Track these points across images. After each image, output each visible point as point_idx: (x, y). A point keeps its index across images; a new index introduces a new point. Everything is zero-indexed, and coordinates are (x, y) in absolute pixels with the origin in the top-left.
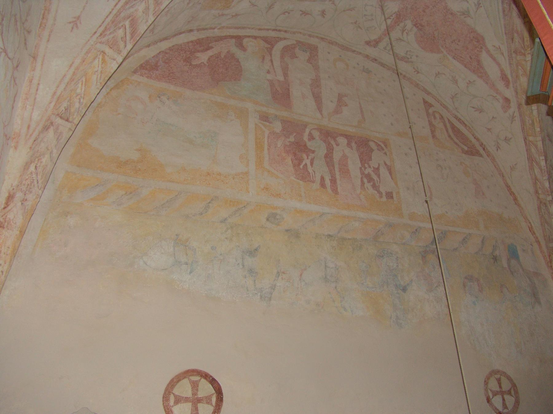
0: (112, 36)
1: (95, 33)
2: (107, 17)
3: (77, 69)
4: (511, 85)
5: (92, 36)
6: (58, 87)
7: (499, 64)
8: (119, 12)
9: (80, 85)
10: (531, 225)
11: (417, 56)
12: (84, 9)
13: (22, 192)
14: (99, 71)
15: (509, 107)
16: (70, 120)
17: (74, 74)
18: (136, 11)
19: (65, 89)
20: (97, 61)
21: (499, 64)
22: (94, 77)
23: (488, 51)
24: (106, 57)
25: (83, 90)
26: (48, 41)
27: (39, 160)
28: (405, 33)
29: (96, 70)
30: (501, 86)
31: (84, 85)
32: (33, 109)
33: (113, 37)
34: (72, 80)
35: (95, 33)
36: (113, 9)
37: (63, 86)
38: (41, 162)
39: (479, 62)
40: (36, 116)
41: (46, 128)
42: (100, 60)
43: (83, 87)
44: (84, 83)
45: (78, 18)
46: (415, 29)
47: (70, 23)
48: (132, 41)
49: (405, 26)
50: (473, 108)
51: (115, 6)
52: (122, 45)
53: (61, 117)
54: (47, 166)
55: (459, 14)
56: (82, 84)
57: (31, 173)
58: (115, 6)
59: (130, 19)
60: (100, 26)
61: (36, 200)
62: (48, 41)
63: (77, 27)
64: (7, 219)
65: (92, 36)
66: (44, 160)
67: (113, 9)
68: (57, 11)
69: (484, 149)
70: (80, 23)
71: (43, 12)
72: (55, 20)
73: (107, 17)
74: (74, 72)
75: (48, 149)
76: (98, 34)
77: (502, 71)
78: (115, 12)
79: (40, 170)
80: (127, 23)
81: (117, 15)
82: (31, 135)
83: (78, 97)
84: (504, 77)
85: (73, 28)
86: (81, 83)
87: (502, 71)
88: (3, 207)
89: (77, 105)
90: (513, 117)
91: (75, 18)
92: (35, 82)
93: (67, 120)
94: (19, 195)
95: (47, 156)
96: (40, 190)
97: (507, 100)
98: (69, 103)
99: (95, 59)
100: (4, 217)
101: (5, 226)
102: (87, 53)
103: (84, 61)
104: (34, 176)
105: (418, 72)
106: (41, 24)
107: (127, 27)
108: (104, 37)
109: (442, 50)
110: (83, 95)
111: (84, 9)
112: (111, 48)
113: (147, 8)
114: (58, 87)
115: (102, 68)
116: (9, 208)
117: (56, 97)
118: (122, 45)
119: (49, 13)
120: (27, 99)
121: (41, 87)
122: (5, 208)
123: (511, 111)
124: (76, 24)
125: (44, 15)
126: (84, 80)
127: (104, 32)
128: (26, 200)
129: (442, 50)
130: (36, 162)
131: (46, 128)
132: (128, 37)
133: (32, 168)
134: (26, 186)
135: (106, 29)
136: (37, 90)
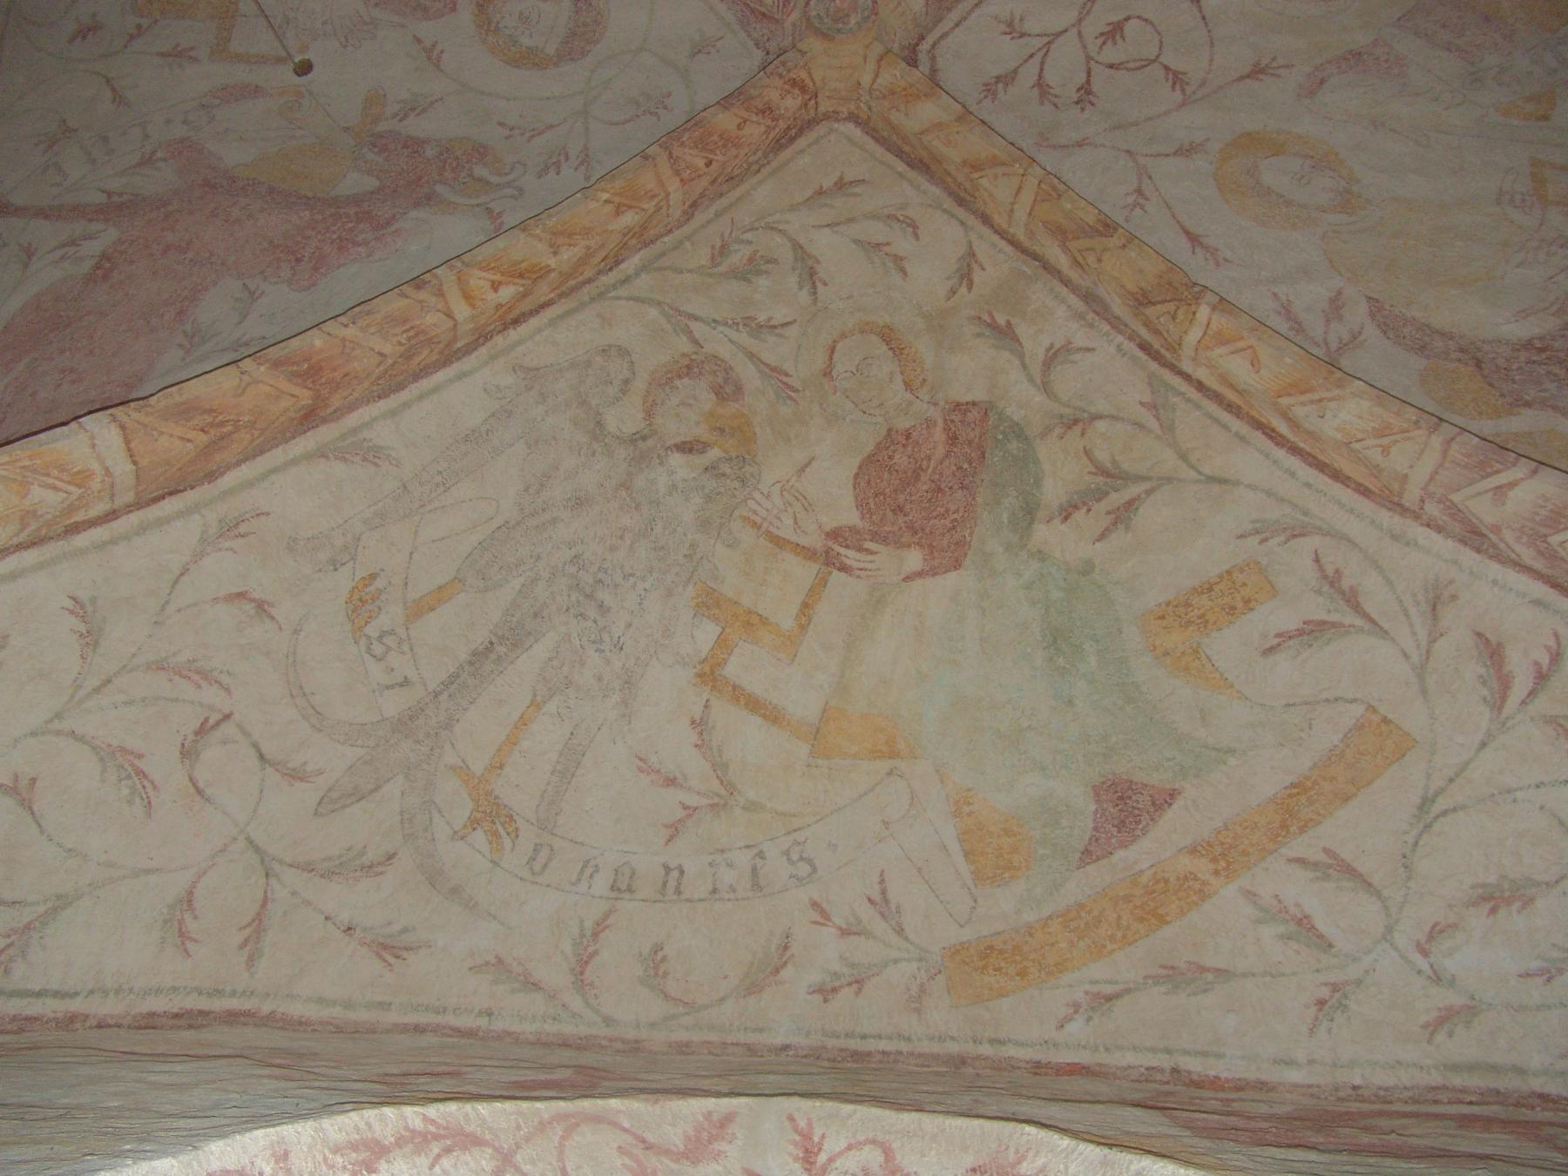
55: (188, 327)
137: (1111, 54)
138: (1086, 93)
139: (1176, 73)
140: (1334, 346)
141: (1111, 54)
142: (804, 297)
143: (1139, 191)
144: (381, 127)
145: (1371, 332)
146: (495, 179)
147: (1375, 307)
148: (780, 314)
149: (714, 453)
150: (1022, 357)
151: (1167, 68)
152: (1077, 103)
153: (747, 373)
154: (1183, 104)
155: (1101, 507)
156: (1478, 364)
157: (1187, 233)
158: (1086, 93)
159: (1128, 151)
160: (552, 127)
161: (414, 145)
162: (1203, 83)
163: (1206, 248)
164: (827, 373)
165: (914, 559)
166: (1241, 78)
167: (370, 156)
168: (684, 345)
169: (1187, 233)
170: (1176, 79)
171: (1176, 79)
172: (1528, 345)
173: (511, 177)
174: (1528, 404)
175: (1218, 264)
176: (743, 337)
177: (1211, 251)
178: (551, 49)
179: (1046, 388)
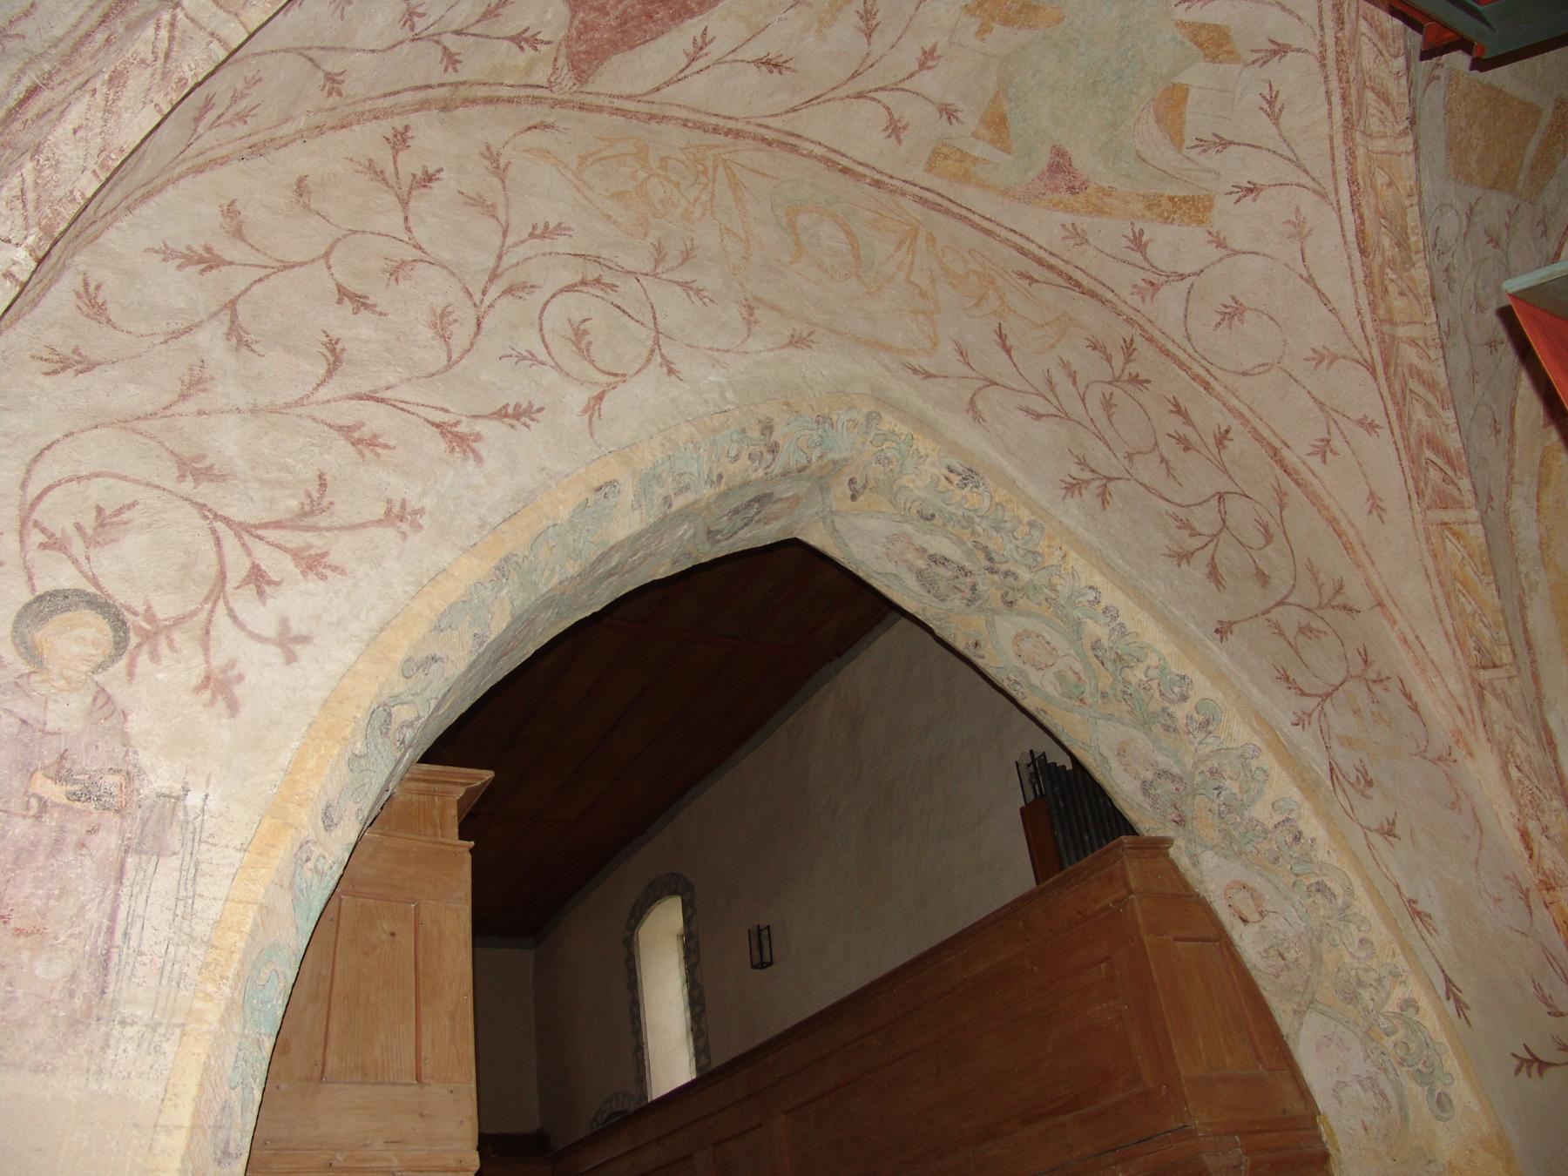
0: (1430, 490)
1: (1409, 498)
2: (1400, 460)
3: (1438, 574)
5: (1411, 507)
6: (1441, 621)
8: (1405, 438)
9: (1463, 600)
12: (1365, 476)
13: (1531, 818)
14: (1466, 556)
16: (1498, 662)
17: (1442, 584)
18: (1419, 423)
19: (1451, 616)
20: (1448, 543)
22: (1469, 571)
24: (1453, 527)
25: (1473, 603)
26: (1373, 563)
27: (1512, 753)
29: (1460, 557)
31: (1467, 595)
32: (1443, 679)
33: (1433, 490)
34: (1447, 596)
35: (1409, 498)
36: (1395, 443)
37: (1446, 615)
38: (1518, 755)
40: (1456, 688)
41: (1481, 698)
42: (1451, 537)
43: (1470, 599)
44: (1464, 591)
45: (1372, 495)
47: (1370, 512)
48: (1459, 474)
51: (1393, 434)
52: (1451, 489)
53: (1484, 668)
54: (1529, 756)
56: (1464, 596)
57: (1519, 781)
58: (1393, 434)
59: (1425, 443)
60: (1406, 481)
61: (1560, 820)
62: (1373, 563)
63: (1383, 510)
64: (1548, 873)
65: (1411, 507)
66: (1518, 749)
67: (1395, 443)
68: (1342, 511)
70: (1381, 500)
71: (1331, 529)
72: (1353, 526)
73: (1400, 460)
74: (1440, 582)
75: (1510, 729)
76: (1414, 497)
78: (1400, 444)
79: (1526, 768)
80: (1428, 453)
81: (1407, 448)
82: (1473, 721)
83: (1477, 620)
85: (1380, 517)
86: (1460, 595)
88: (1527, 856)
89: (1486, 632)
91: (1368, 500)
92: (1410, 637)
93: (1495, 666)
94: (1532, 825)
95: (1517, 740)
96: (1551, 800)
98: (1474, 638)
99: (1443, 542)
100: (1541, 871)
101: (1554, 885)
102: (1428, 539)
103: (1436, 556)
104: (1527, 783)
106: (1346, 548)
107: (1433, 458)
108: (1424, 496)
110: (1480, 612)
111: (1365, 476)
112: (1446, 508)
113: (1428, 406)
114: (1441, 621)
115: (1465, 547)
116: (1536, 853)
117: (1452, 638)
118: (1451, 489)
119: (1338, 524)
120: (1423, 670)
121: (1424, 639)
122: (1531, 857)
124: (1378, 506)
125: (1336, 532)
126: (1461, 587)
127: (1416, 487)
128: (1547, 828)
130: (1512, 760)
131: (1481, 698)
132: (1451, 473)
133: (1515, 773)
134: (1529, 806)
135: (1416, 480)
136: (1423, 646)
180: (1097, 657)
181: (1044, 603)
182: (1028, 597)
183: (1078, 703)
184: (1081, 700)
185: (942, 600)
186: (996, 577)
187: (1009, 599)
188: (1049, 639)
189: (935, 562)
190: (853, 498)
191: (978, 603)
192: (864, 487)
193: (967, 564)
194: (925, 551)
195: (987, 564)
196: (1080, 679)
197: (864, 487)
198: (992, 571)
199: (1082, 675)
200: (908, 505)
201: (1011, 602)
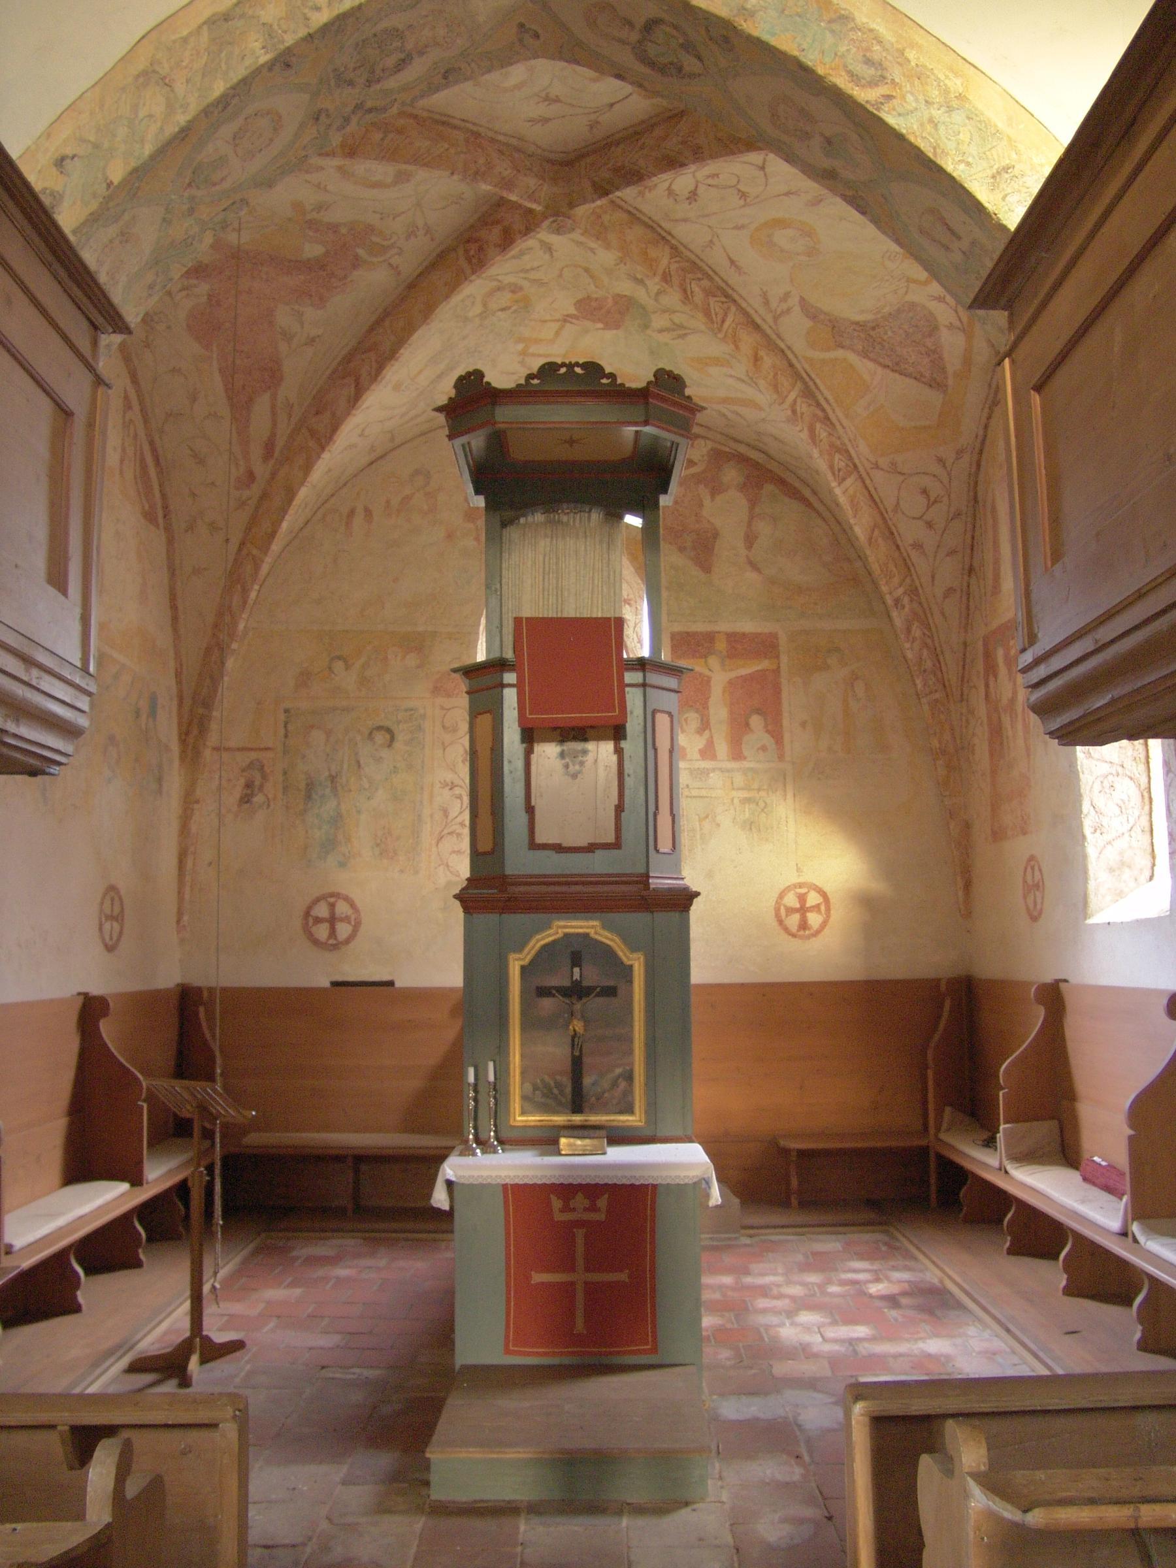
4: (272, 462)
7: (274, 424)
10: (181, 669)
11: (169, 327)
15: (248, 486)
21: (274, 424)
23: (274, 398)
28: (184, 293)
30: (256, 451)
39: (251, 400)
46: (204, 299)
49: (195, 286)
50: (192, 450)
69: (165, 516)
77: (273, 435)
84: (269, 448)
87: (273, 435)
90: (244, 503)
97: (251, 476)
105: (147, 346)
109: (215, 349)
123: (246, 493)
129: (215, 349)
137: (710, 181)
138: (693, 196)
139: (743, 193)
140: (778, 313)
141: (710, 181)
142: (547, 257)
143: (711, 241)
144: (309, 217)
145: (797, 309)
146: (386, 243)
147: (802, 299)
148: (536, 264)
149: (514, 308)
150: (647, 289)
151: (739, 190)
152: (688, 199)
153: (525, 284)
154: (744, 206)
155: (675, 333)
156: (834, 327)
157: (730, 258)
158: (693, 196)
159: (709, 226)
160: (403, 213)
161: (334, 228)
162: (758, 197)
163: (737, 267)
164: (560, 276)
165: (600, 325)
166: (779, 196)
167: (311, 233)
168: (495, 284)
169: (730, 258)
170: (743, 195)
171: (743, 195)
172: (857, 323)
173: (392, 241)
174: (842, 347)
175: (740, 274)
176: (522, 275)
177: (738, 268)
178: (389, 180)
179: (656, 300)
180: (234, 203)
181: (304, 153)
182: (317, 138)
183: (187, 181)
184: (189, 185)
185: (357, 44)
186: (349, 109)
187: (323, 118)
188: (263, 152)
189: (403, 60)
190: (521, 25)
191: (333, 83)
192: (521, 40)
193: (378, 87)
194: (421, 53)
195: (369, 104)
196: (214, 185)
197: (521, 40)
198: (358, 107)
199: (218, 188)
200: (473, 65)
201: (317, 119)
